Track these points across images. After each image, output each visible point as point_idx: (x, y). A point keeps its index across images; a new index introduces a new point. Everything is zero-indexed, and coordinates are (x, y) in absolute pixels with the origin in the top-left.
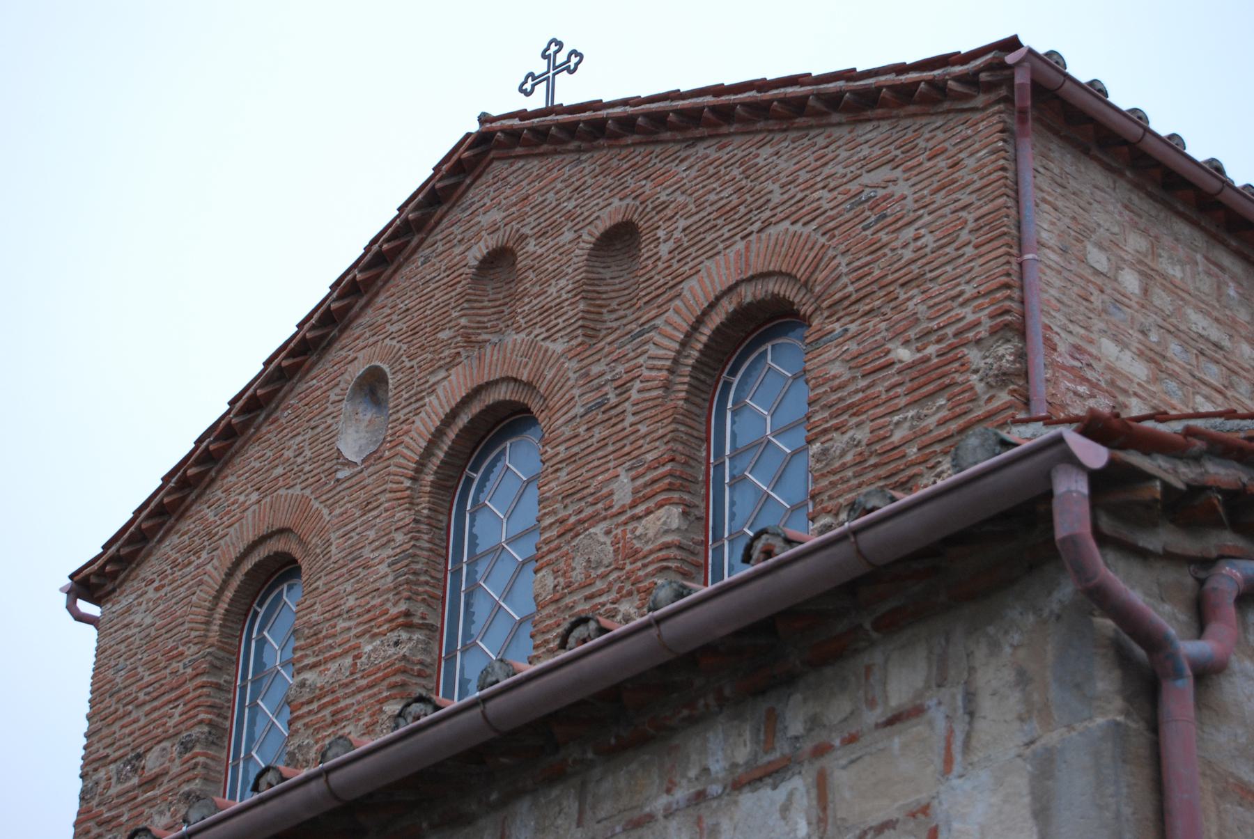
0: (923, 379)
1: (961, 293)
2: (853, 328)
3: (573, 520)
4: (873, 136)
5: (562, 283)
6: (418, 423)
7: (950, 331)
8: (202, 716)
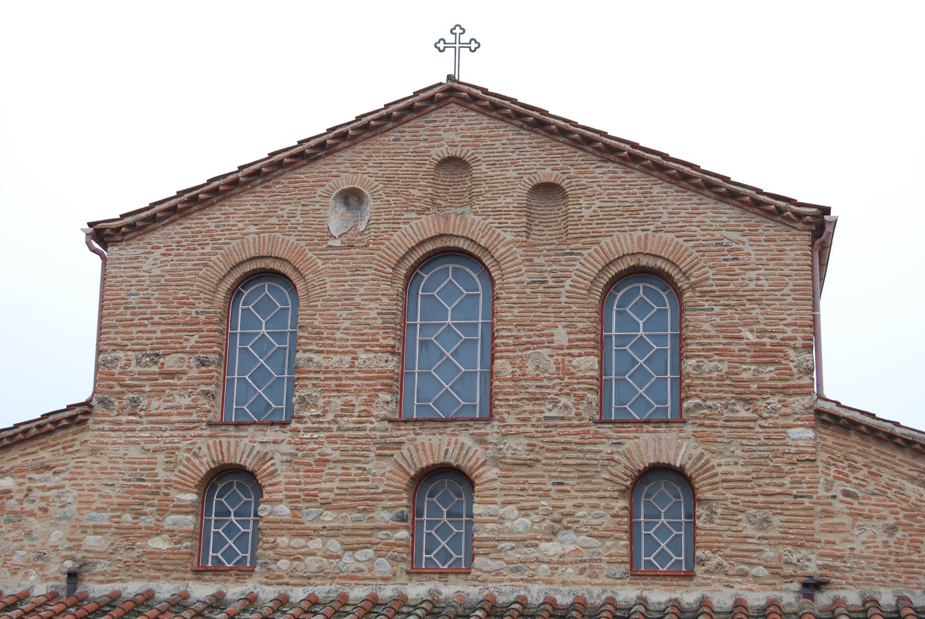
0: (762, 354)
1: (785, 319)
2: (717, 309)
3: (524, 339)
4: (729, 213)
5: (509, 200)
6: (395, 236)
7: (779, 336)
8: (215, 349)
